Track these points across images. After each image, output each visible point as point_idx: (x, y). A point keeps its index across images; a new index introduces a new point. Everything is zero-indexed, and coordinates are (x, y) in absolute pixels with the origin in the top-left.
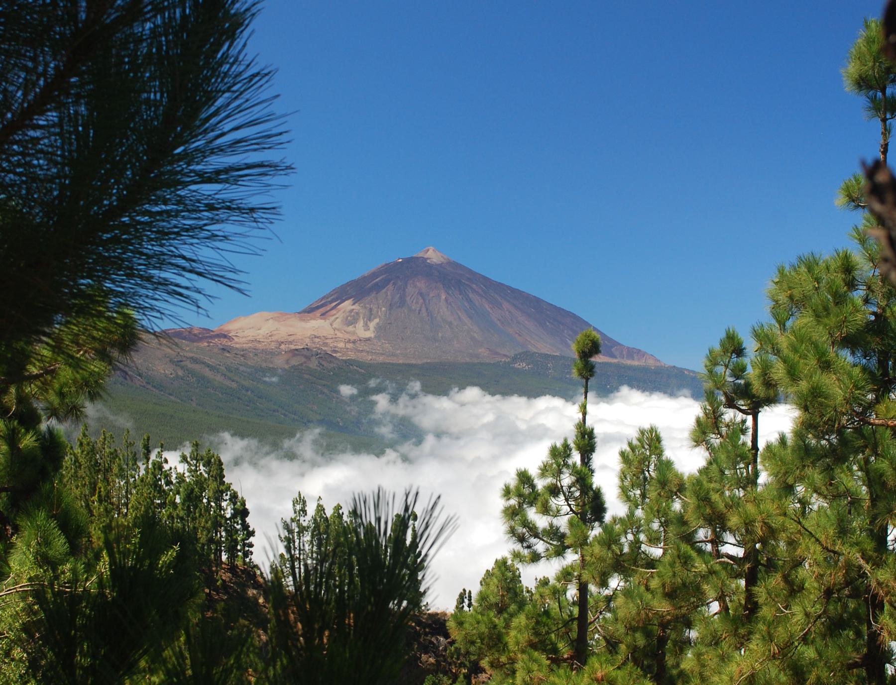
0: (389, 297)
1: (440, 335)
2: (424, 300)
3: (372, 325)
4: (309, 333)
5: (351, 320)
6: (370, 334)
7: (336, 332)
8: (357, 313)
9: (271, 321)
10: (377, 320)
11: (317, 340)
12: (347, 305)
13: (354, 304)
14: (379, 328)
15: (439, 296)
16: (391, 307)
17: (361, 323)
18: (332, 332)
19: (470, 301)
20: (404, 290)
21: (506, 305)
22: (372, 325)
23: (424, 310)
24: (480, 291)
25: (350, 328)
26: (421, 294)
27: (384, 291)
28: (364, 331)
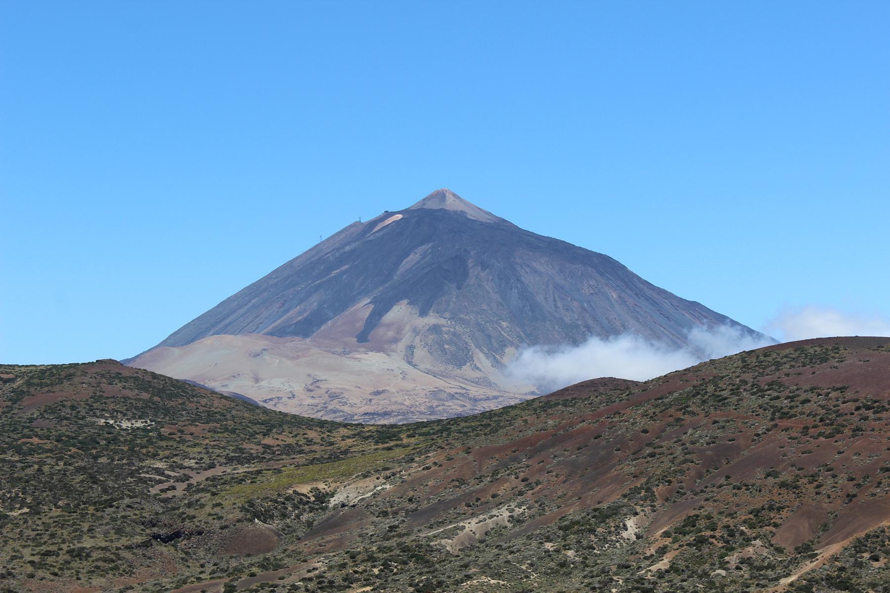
13: (423, 313)
17: (482, 360)
20: (518, 280)
25: (467, 370)
27: (472, 281)
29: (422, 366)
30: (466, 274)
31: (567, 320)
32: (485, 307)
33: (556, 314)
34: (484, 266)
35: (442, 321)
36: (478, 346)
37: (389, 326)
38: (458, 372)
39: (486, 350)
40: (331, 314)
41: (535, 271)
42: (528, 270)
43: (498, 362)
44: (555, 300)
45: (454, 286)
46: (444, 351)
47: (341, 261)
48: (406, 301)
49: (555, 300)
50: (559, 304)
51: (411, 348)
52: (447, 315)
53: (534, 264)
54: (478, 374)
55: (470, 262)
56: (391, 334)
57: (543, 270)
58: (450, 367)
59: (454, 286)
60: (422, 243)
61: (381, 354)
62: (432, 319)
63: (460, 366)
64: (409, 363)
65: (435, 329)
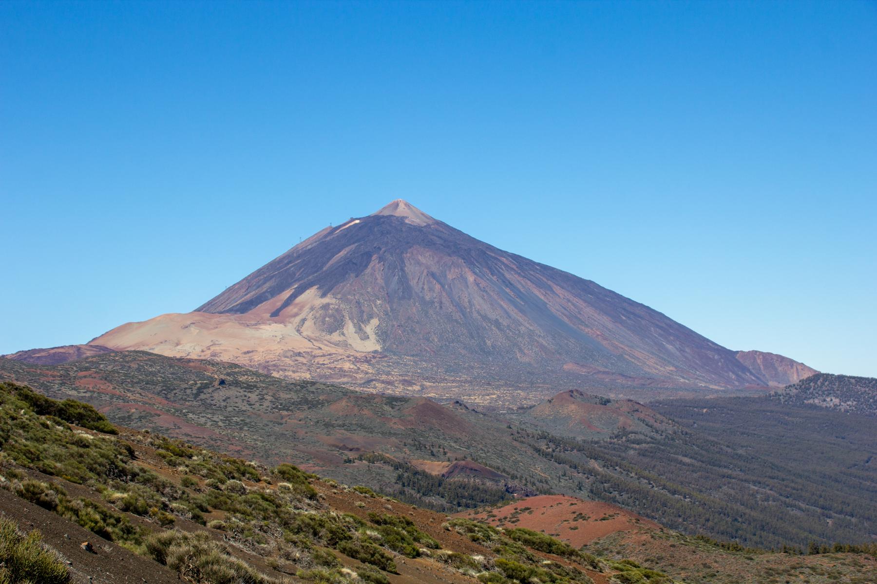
0: (380, 281)
1: (489, 343)
2: (443, 286)
3: (370, 329)
4: (278, 348)
5: (332, 323)
6: (372, 345)
7: (317, 344)
8: (337, 310)
9: (194, 330)
10: (375, 322)
11: (300, 359)
12: (311, 297)
13: (324, 295)
14: (383, 335)
16: (389, 298)
17: (350, 328)
19: (509, 284)
20: (402, 270)
21: (557, 289)
22: (370, 329)
23: (446, 301)
24: (514, 267)
25: (336, 337)
26: (433, 275)
27: (369, 270)
29: (305, 334)
30: (366, 266)
31: (427, 298)
32: (369, 290)
33: (421, 295)
34: (381, 259)
35: (334, 301)
36: (351, 319)
37: (297, 304)
38: (328, 337)
39: (356, 321)
40: (269, 296)
41: (419, 263)
42: (412, 262)
43: (361, 329)
44: (424, 284)
45: (353, 275)
46: (323, 322)
47: (299, 257)
48: (316, 287)
49: (424, 284)
50: (426, 287)
51: (304, 320)
52: (339, 296)
53: (420, 257)
54: (342, 338)
55: (374, 257)
56: (295, 310)
57: (424, 262)
58: (324, 334)
59: (353, 275)
60: (354, 243)
61: (282, 325)
63: (331, 333)
64: (298, 331)
65: (325, 307)
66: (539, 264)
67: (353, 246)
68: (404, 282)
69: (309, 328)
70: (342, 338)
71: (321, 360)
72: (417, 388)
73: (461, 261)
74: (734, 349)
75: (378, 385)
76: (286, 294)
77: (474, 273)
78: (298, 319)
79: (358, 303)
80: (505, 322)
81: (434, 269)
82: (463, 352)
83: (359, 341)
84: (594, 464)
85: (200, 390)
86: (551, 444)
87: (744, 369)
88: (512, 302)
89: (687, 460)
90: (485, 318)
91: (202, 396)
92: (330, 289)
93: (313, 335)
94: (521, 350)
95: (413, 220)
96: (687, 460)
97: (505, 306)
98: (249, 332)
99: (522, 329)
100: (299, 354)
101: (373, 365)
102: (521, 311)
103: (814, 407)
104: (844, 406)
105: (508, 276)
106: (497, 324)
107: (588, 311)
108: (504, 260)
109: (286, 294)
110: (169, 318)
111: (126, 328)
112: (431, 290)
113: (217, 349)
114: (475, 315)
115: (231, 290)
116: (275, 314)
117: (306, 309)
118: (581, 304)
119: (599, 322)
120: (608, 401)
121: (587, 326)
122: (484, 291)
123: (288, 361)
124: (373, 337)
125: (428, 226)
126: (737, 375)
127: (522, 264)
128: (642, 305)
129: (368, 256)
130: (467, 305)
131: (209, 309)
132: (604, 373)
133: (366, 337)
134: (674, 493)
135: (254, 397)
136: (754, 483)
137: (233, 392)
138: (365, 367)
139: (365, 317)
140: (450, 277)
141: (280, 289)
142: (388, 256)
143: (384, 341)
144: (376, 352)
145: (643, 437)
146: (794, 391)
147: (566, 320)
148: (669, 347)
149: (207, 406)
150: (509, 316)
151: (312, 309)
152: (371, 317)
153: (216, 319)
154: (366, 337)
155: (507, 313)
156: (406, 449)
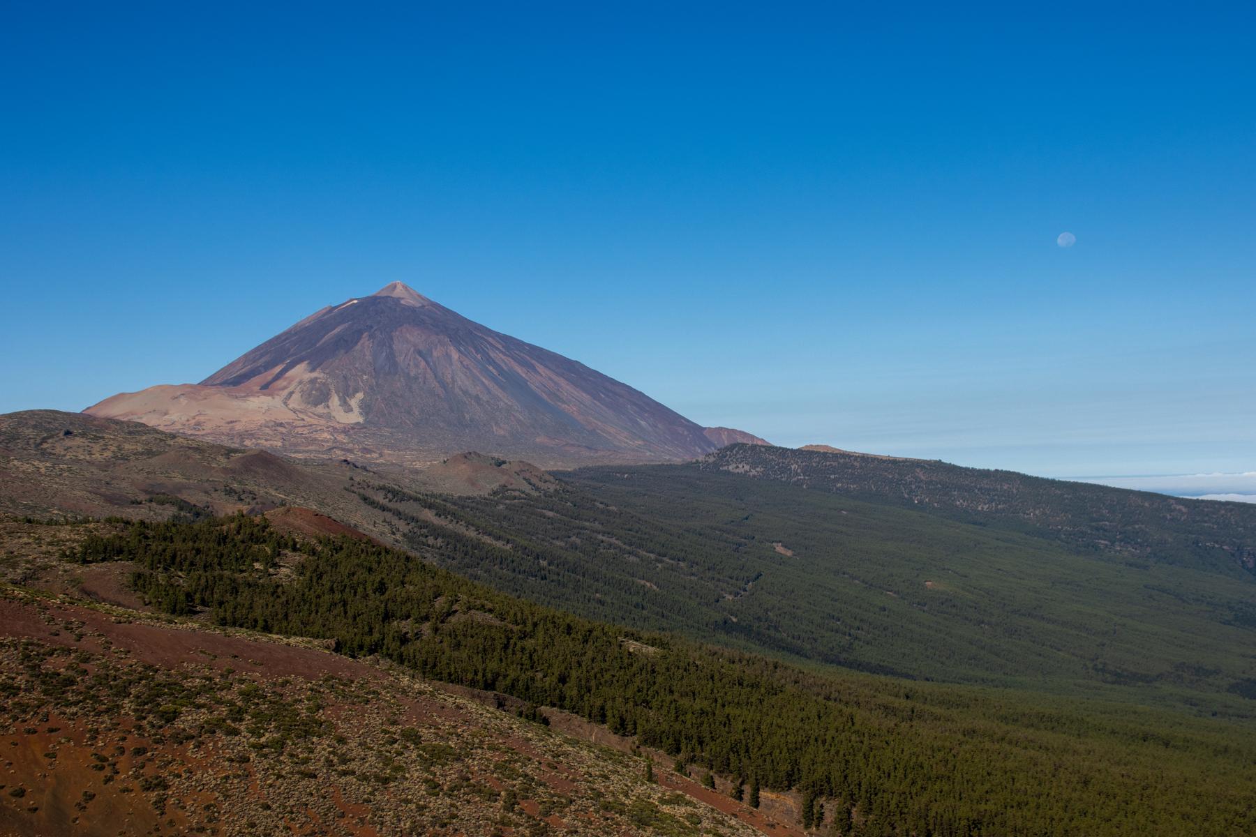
0: (369, 358)
1: (467, 417)
2: (427, 363)
4: (260, 419)
5: (318, 396)
6: (355, 417)
7: (301, 416)
9: (183, 401)
10: (360, 395)
12: (300, 372)
13: (313, 370)
14: (366, 408)
15: (448, 356)
17: (335, 401)
18: (294, 416)
20: (391, 347)
22: (354, 403)
23: (430, 375)
25: (320, 409)
26: (420, 353)
27: (358, 347)
28: (347, 414)
30: (356, 343)
31: (412, 374)
34: (371, 337)
45: (342, 351)
46: (309, 395)
51: (291, 393)
54: (326, 411)
59: (342, 351)
62: (314, 375)
63: (316, 405)
65: (313, 381)
66: (529, 345)
67: (346, 325)
68: (391, 356)
69: (295, 402)
70: (326, 411)
71: (300, 430)
72: (374, 455)
73: (447, 340)
74: (703, 423)
75: (338, 452)
76: (278, 369)
77: (460, 351)
78: (286, 392)
79: (345, 377)
80: (485, 398)
81: (421, 347)
82: (442, 425)
83: (342, 413)
84: (429, 515)
85: (44, 440)
86: (390, 496)
87: (710, 444)
88: (493, 379)
89: (551, 514)
90: (465, 392)
91: (45, 446)
92: (319, 365)
93: (298, 408)
94: (497, 424)
95: (410, 302)
96: (551, 514)
97: (486, 382)
98: (236, 403)
99: (501, 404)
100: (281, 425)
101: (350, 436)
102: (502, 388)
103: (728, 472)
104: (753, 472)
105: (492, 354)
106: (477, 399)
107: (566, 388)
108: (490, 339)
109: (278, 369)
110: (162, 389)
111: (120, 397)
112: (417, 366)
113: (202, 419)
114: (457, 390)
115: (232, 365)
116: (265, 387)
117: (294, 384)
118: (562, 382)
119: (574, 399)
120: (504, 462)
121: (564, 402)
122: (468, 368)
123: (267, 431)
124: (356, 410)
125: (423, 306)
126: (703, 449)
127: (510, 344)
128: (624, 385)
129: (360, 332)
130: (449, 380)
131: (205, 384)
132: (573, 445)
133: (349, 410)
134: (499, 538)
135: (96, 448)
136: (604, 533)
137: (78, 441)
138: (342, 438)
139: (351, 390)
140: (435, 354)
141: (275, 365)
142: (378, 333)
143: (367, 414)
144: (358, 424)
145: (517, 494)
146: (711, 460)
147: (545, 396)
148: (643, 423)
149: (45, 455)
150: (489, 391)
151: (300, 382)
152: (356, 391)
153: (207, 391)
154: (349, 410)
155: (488, 389)
156: (214, 495)
